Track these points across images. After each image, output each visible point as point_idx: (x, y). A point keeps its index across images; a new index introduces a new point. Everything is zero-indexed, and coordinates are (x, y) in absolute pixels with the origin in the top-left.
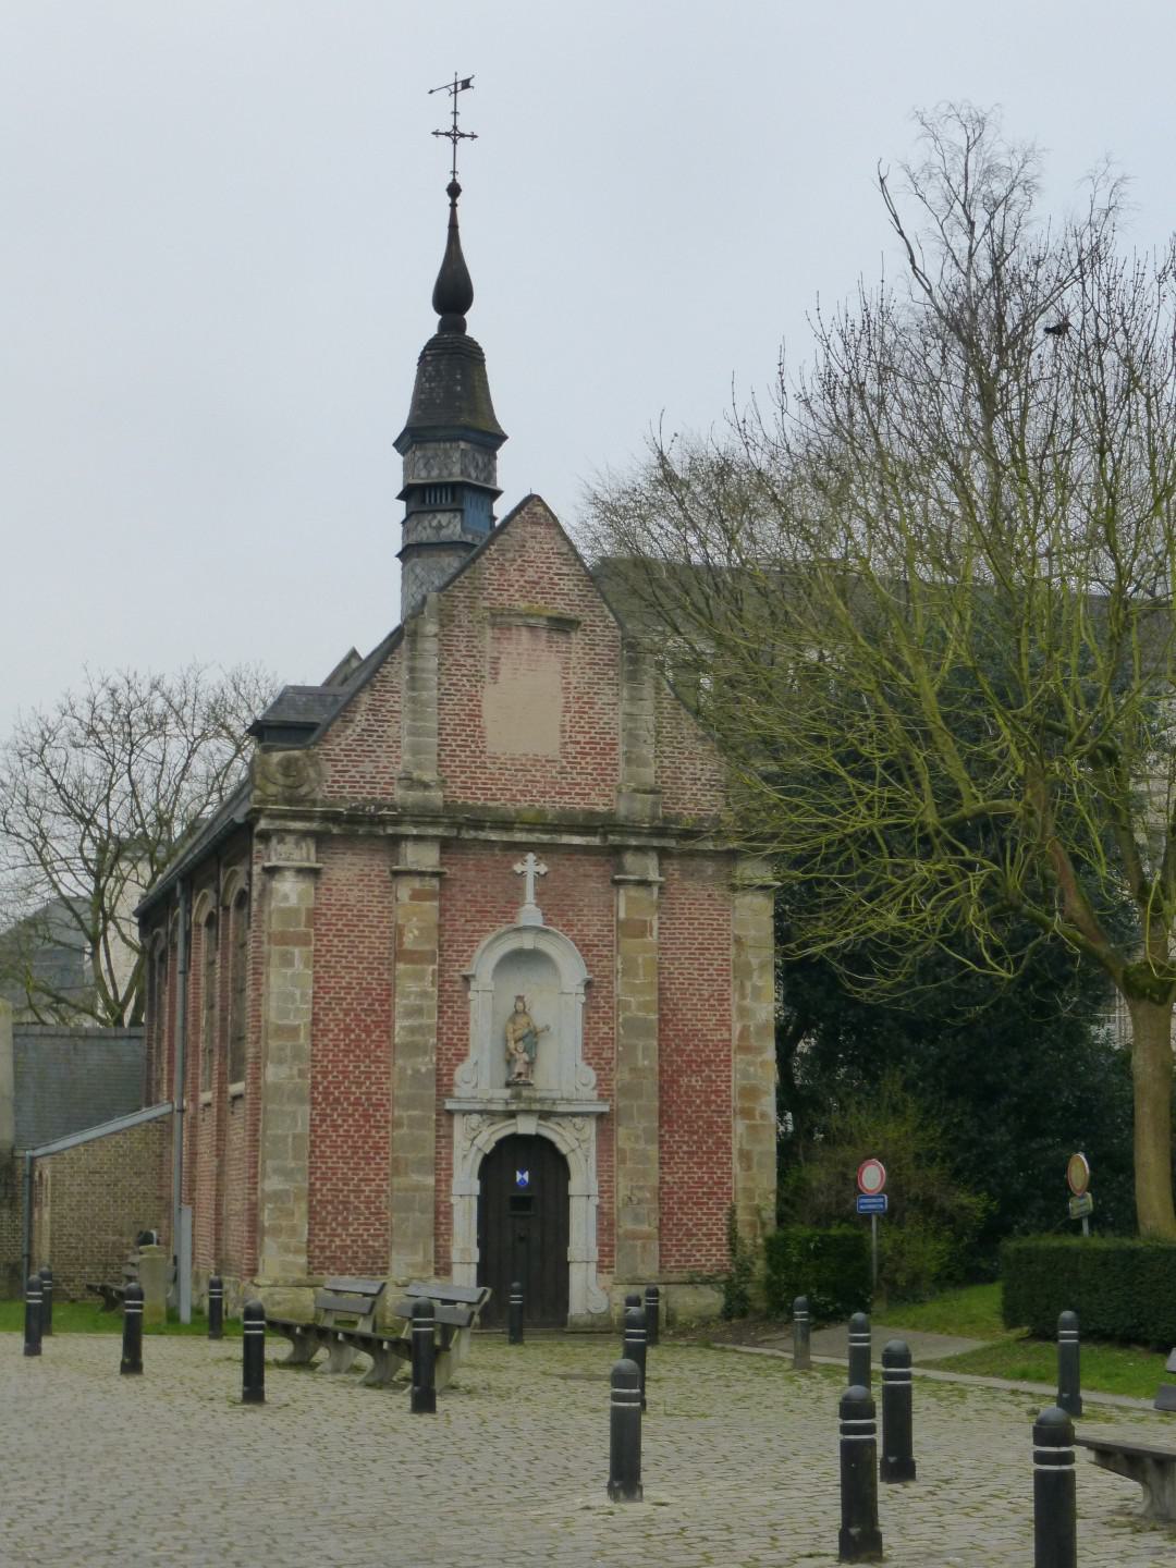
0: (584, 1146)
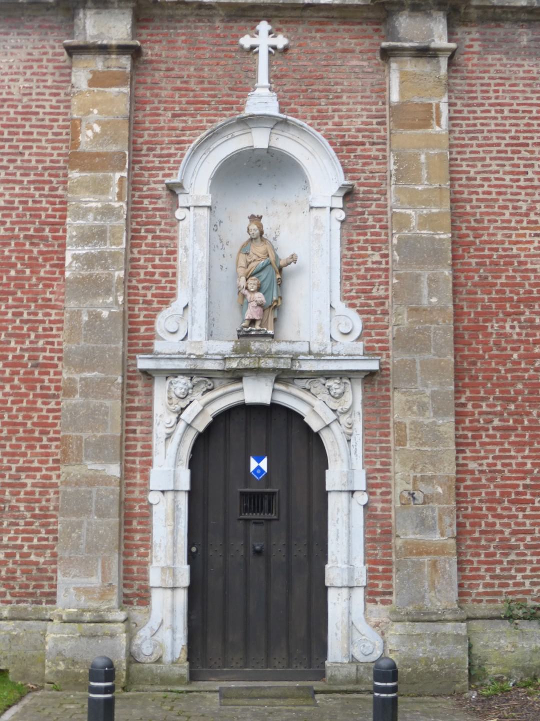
0: (344, 419)
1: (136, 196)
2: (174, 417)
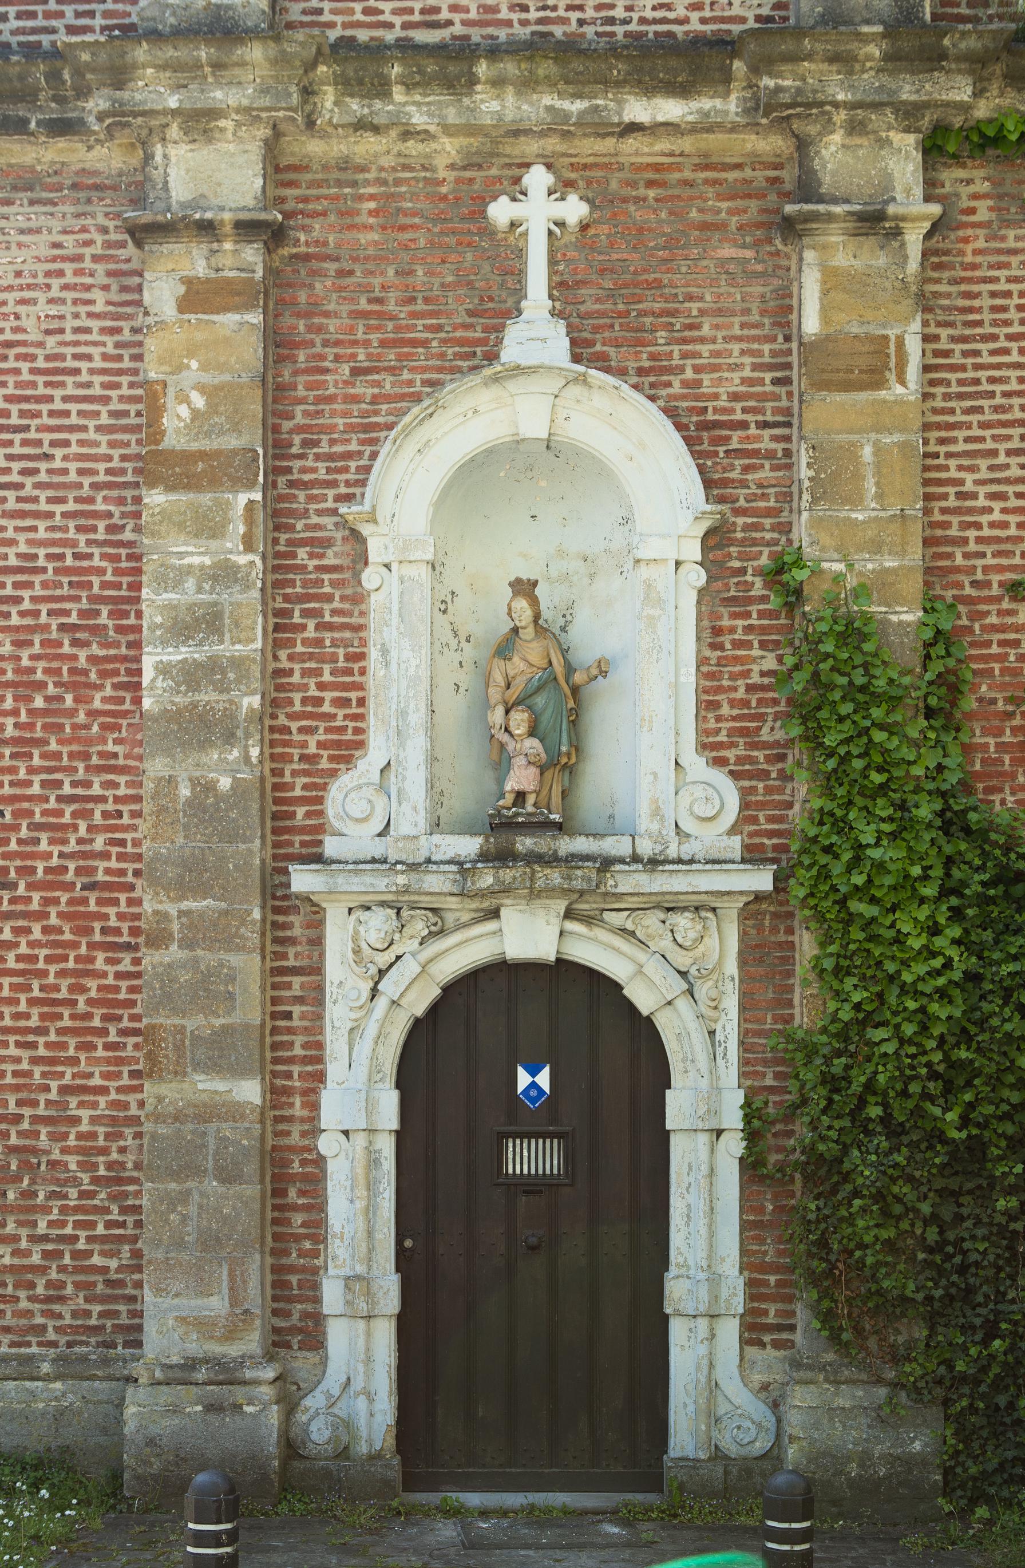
1: (282, 541)
2: (366, 986)
